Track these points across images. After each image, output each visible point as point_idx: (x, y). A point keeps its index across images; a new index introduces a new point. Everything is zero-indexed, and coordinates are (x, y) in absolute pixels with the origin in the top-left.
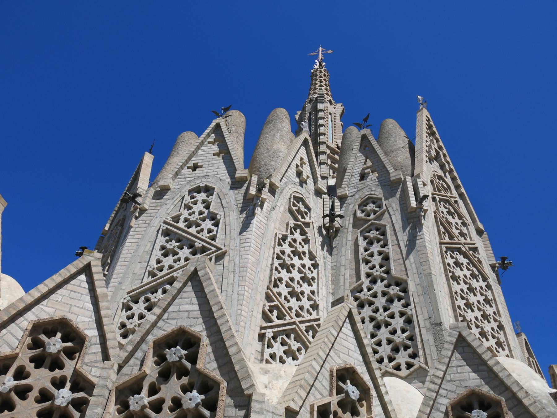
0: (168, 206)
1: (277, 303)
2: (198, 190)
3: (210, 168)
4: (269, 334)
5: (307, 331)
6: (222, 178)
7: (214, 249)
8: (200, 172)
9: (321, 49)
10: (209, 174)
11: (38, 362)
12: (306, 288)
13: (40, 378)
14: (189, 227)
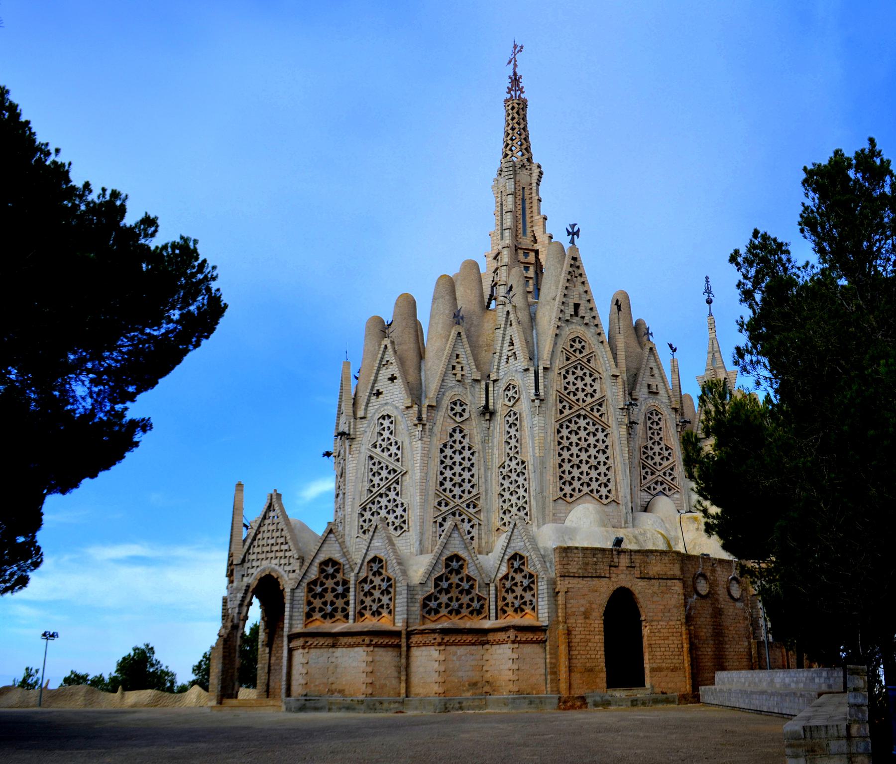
1: (443, 497)
2: (383, 417)
4: (440, 520)
5: (468, 506)
14: (383, 451)
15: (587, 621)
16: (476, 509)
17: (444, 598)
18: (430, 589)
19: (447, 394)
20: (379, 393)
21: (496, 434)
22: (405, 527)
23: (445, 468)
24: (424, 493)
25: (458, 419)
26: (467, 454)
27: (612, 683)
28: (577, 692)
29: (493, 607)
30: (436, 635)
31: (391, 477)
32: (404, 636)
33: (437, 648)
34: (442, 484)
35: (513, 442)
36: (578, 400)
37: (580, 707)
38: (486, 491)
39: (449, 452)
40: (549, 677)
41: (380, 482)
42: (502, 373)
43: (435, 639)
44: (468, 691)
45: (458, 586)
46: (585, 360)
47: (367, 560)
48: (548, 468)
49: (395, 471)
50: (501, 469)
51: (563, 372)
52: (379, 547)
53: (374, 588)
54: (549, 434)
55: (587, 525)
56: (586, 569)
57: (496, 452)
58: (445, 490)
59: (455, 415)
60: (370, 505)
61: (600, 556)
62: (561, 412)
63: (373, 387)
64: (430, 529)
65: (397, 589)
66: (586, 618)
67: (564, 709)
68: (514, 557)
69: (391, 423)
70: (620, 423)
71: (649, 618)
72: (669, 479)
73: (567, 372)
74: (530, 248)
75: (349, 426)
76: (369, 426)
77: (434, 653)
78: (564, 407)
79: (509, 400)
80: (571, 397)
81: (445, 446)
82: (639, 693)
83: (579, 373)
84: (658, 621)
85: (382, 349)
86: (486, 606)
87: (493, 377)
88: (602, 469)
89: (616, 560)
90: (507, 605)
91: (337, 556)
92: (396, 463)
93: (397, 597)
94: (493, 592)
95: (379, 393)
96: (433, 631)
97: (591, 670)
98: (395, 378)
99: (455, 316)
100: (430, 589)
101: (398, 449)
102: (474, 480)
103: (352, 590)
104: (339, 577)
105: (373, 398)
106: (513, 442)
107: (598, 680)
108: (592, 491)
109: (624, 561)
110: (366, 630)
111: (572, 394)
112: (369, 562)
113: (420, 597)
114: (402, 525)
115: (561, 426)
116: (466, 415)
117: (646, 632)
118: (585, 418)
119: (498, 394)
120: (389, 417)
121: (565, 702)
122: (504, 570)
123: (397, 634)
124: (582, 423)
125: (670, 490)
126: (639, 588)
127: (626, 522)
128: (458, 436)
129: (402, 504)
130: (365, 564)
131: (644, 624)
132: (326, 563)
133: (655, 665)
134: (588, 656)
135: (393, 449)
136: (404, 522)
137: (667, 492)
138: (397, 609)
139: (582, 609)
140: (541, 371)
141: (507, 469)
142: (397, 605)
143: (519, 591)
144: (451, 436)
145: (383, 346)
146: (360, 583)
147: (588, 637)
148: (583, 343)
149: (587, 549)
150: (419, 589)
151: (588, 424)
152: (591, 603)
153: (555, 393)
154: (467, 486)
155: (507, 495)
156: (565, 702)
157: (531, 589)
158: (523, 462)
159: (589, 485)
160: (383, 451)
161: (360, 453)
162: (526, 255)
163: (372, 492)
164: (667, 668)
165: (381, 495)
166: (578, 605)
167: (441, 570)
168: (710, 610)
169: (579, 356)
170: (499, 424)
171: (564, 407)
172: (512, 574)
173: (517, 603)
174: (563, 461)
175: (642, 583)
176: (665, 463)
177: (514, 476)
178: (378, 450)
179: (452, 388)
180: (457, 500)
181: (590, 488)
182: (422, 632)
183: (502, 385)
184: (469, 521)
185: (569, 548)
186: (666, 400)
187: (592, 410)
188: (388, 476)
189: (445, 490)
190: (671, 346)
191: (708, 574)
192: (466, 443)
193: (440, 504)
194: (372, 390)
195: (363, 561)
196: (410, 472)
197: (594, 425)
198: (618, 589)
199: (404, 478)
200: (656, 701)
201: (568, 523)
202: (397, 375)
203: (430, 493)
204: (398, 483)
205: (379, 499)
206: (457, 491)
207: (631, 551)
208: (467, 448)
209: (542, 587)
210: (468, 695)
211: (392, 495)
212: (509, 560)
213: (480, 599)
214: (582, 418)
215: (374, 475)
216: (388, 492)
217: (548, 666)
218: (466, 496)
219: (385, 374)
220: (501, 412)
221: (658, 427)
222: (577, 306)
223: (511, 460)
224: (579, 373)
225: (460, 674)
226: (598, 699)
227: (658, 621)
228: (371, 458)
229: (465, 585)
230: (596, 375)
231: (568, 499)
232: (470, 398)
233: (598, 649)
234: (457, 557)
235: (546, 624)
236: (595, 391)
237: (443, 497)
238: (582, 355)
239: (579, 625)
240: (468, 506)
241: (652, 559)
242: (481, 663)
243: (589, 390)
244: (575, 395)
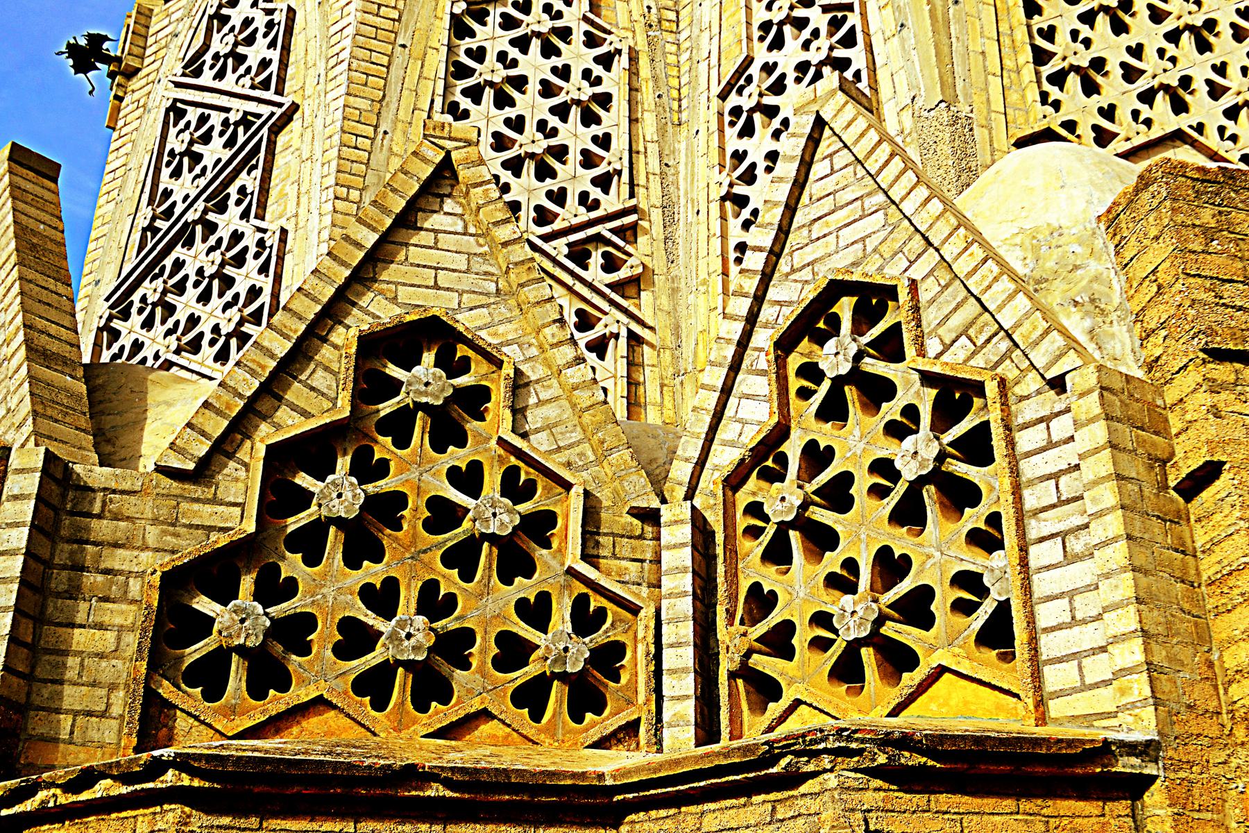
0: (181, 37)
17: (329, 588)
29: (680, 658)
45: (443, 515)
86: (636, 664)
102: (615, 158)
154: (573, 176)
157: (961, 495)
167: (322, 397)
172: (807, 427)
173: (854, 614)
209: (1061, 461)
235: (1142, 727)
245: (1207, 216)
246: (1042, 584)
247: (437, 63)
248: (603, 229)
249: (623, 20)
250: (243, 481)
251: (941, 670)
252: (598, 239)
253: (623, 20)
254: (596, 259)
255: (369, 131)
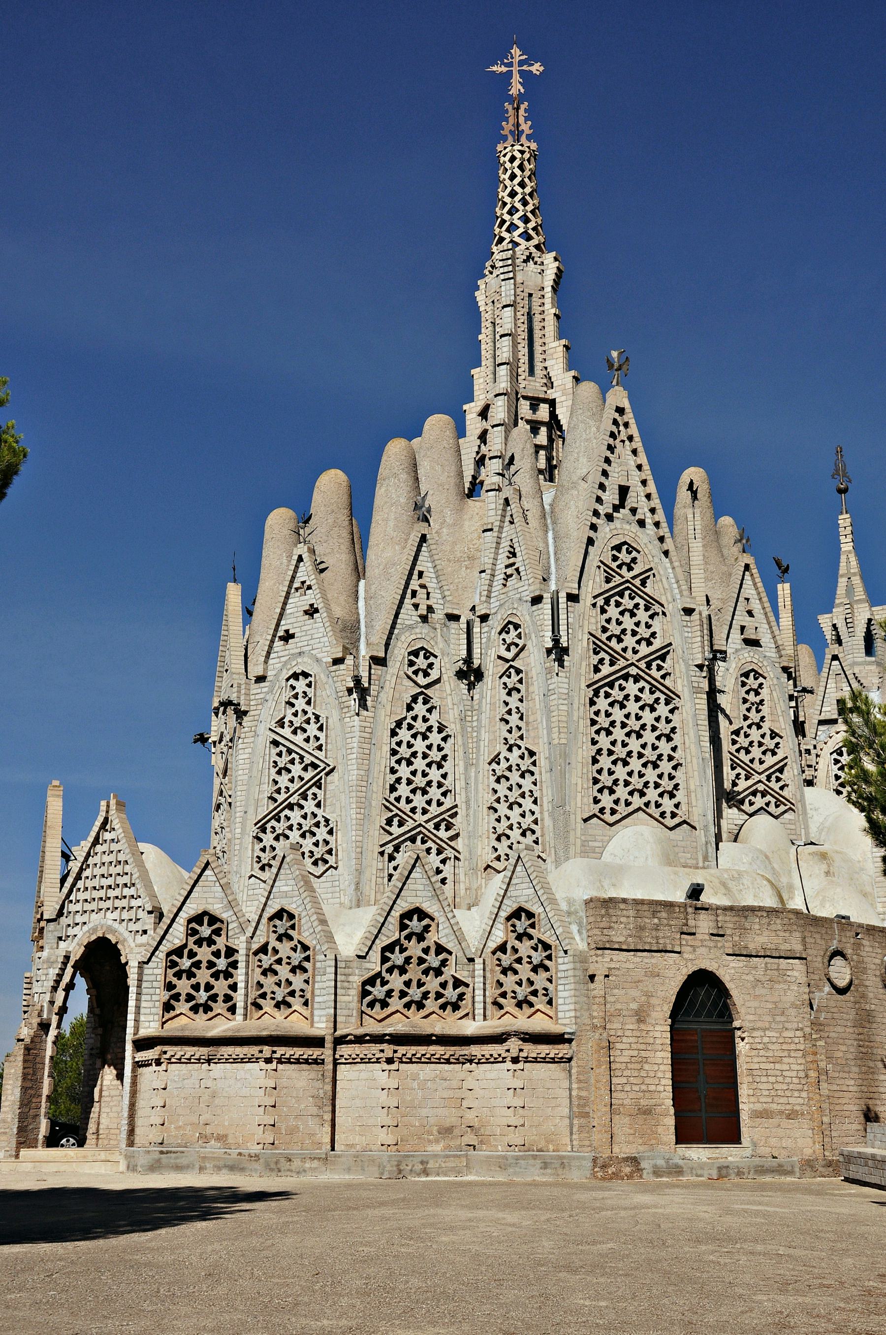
2: (295, 676)
3: (303, 639)
4: (389, 849)
5: (437, 827)
6: (319, 656)
7: (322, 765)
8: (293, 646)
9: (516, 51)
10: (304, 649)
11: (199, 942)
12: (435, 774)
13: (204, 953)
14: (295, 732)
15: (643, 1026)
16: (451, 833)
17: (396, 982)
18: (374, 965)
19: (403, 638)
20: (288, 637)
21: (486, 708)
22: (332, 860)
23: (399, 762)
24: (363, 804)
25: (421, 680)
26: (435, 738)
27: (685, 1134)
28: (622, 1150)
29: (479, 998)
30: (384, 1046)
31: (307, 776)
32: (329, 1044)
33: (385, 1066)
34: (393, 789)
35: (514, 719)
36: (625, 650)
37: (630, 1177)
38: (467, 802)
39: (404, 735)
40: (576, 1121)
41: (290, 785)
42: (494, 603)
43: (382, 1051)
44: (437, 1141)
45: (421, 961)
46: (637, 582)
47: (266, 915)
48: (573, 765)
49: (314, 766)
50: (494, 766)
51: (600, 601)
52: (287, 894)
53: (279, 962)
54: (575, 706)
55: (638, 862)
56: (640, 938)
57: (485, 736)
58: (398, 799)
59: (416, 673)
60: (273, 823)
61: (664, 915)
62: (597, 670)
63: (278, 625)
64: (375, 865)
65: (318, 965)
66: (640, 1021)
67: (603, 1179)
68: (517, 914)
69: (309, 685)
70: (696, 690)
71: (747, 1025)
72: (776, 786)
73: (607, 601)
74: (542, 396)
75: (239, 692)
76: (271, 691)
77: (378, 1073)
78: (601, 661)
79: (508, 649)
80: (613, 643)
81: (399, 724)
82: (728, 1153)
83: (627, 603)
84: (765, 1030)
85: (294, 562)
86: (468, 997)
87: (481, 611)
88: (666, 767)
89: (691, 922)
90: (504, 995)
91: (217, 909)
92: (317, 753)
93: (318, 978)
94: (479, 972)
95: (288, 637)
96: (377, 1039)
97: (647, 1112)
98: (317, 611)
99: (417, 507)
100: (374, 965)
101: (321, 729)
103: (241, 965)
104: (221, 943)
105: (278, 644)
106: (514, 719)
107: (660, 1129)
108: (647, 804)
109: (704, 924)
110: (265, 1033)
111: (614, 640)
112: (271, 919)
113: (357, 980)
114: (327, 857)
115: (596, 693)
116: (434, 674)
117: (741, 1047)
118: (636, 681)
119: (489, 638)
120: (306, 675)
121: (604, 1167)
122: (499, 935)
123: (318, 1042)
124: (632, 688)
125: (777, 806)
126: (729, 971)
127: (706, 858)
128: (420, 709)
129: (327, 821)
130: (264, 921)
131: (738, 1033)
132: (198, 919)
133: (758, 1107)
134: (644, 1087)
135: (312, 730)
136: (330, 852)
137: (772, 808)
138: (317, 999)
139: (634, 1006)
140: (563, 600)
141: (504, 765)
142: (317, 992)
143: (524, 971)
144: (409, 708)
145: (296, 557)
146: (256, 953)
147: (643, 1054)
148: (634, 554)
149: (642, 902)
150: (355, 964)
151: (641, 690)
152: (648, 995)
153: (586, 636)
154: (435, 793)
155: (503, 809)
156: (604, 1167)
158: (532, 754)
159: (642, 794)
160: (295, 732)
161: (256, 735)
162: (534, 408)
163: (275, 800)
164: (781, 1112)
165: (290, 807)
166: (626, 998)
167: (392, 933)
168: (852, 1014)
169: (628, 575)
170: (491, 688)
171: (601, 661)
172: (512, 942)
174: (599, 752)
175: (737, 963)
176: (770, 760)
177: (515, 777)
178: (287, 732)
179: (411, 627)
180: (420, 818)
181: (645, 799)
182: (360, 1040)
183: (496, 623)
184: (439, 852)
185: (611, 899)
186: (772, 654)
187: (649, 665)
188: (303, 774)
189: (398, 799)
190: (778, 563)
191: (849, 951)
192: (433, 719)
193: (389, 822)
194: (276, 630)
195: (261, 916)
196: (339, 768)
197: (652, 693)
198: (694, 972)
199: (329, 778)
200: (761, 1170)
201: (606, 857)
202: (319, 605)
203: (374, 803)
204: (320, 788)
205: (287, 812)
206: (419, 801)
207: (718, 908)
208: (435, 729)
210: (437, 1148)
211: (309, 806)
212: (508, 919)
213: (458, 983)
214: (631, 680)
215: (279, 773)
216: (302, 802)
217: (575, 1102)
218: (434, 810)
219: (298, 602)
220: (492, 669)
221: (758, 699)
222: (624, 491)
223: (510, 750)
224: (627, 603)
225: (424, 1112)
226: (661, 1162)
227: (765, 1030)
228: (275, 743)
229: (433, 960)
230: (657, 608)
231: (607, 816)
232: (441, 644)
233: (660, 1075)
234: (422, 914)
236: (653, 635)
237: (396, 811)
238: (632, 574)
239: (628, 1033)
240: (437, 827)
241: (755, 922)
242: (459, 1094)
243: (644, 632)
244: (620, 640)
245: (603, 912)
246: (560, 994)
247: (386, 749)
248: (445, 816)
249: (452, 720)
250: (375, 956)
251: (538, 1010)
252: (444, 819)
253: (452, 720)
254: (443, 827)
255: (364, 784)
